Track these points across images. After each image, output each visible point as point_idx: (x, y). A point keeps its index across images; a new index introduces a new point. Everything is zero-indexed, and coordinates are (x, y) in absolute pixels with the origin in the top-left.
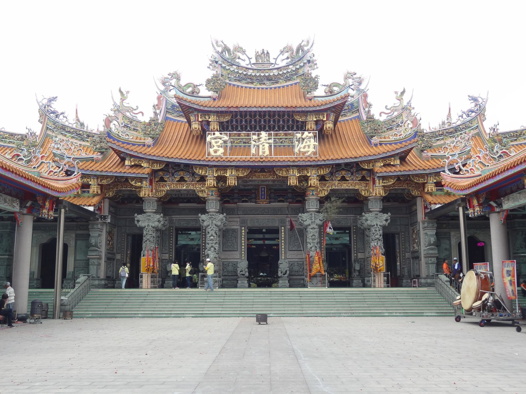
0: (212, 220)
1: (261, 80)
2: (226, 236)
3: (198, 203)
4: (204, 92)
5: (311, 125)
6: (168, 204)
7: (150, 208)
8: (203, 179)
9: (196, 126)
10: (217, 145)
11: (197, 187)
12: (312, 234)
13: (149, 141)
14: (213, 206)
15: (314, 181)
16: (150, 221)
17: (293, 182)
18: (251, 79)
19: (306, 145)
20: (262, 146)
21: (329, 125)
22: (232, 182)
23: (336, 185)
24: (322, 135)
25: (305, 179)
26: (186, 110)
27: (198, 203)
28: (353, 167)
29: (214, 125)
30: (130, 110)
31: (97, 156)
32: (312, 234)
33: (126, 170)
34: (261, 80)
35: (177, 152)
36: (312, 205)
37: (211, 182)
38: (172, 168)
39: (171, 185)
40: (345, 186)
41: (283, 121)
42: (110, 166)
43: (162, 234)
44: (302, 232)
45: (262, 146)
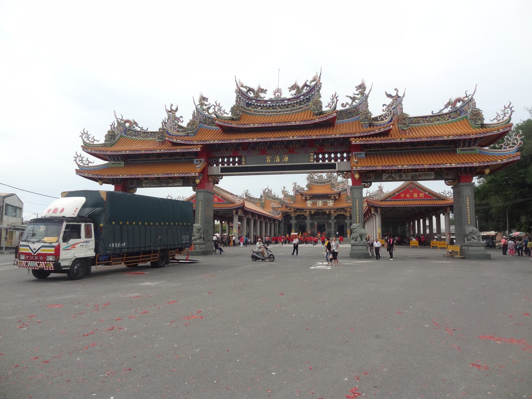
0: (308, 222)
1: (321, 183)
2: (312, 225)
3: (305, 218)
4: (306, 189)
5: (332, 198)
6: (298, 217)
7: (293, 219)
8: (306, 212)
9: (304, 198)
10: (309, 204)
11: (304, 214)
12: (333, 225)
13: (292, 202)
14: (308, 218)
15: (332, 213)
16: (293, 222)
17: (327, 213)
18: (318, 183)
19: (331, 203)
20: (320, 204)
21: (337, 198)
22: (313, 213)
23: (339, 213)
24: (335, 200)
25: (330, 212)
26: (302, 195)
27: (305, 218)
28: (343, 209)
29: (308, 198)
30: (286, 191)
31: (280, 206)
32: (333, 225)
33: (287, 210)
34: (321, 183)
35: (299, 206)
36: (333, 218)
37: (308, 213)
38: (298, 209)
39: (298, 213)
40: (341, 213)
41: (326, 197)
42: (284, 209)
43: (296, 225)
44: (330, 224)
45: (320, 204)
